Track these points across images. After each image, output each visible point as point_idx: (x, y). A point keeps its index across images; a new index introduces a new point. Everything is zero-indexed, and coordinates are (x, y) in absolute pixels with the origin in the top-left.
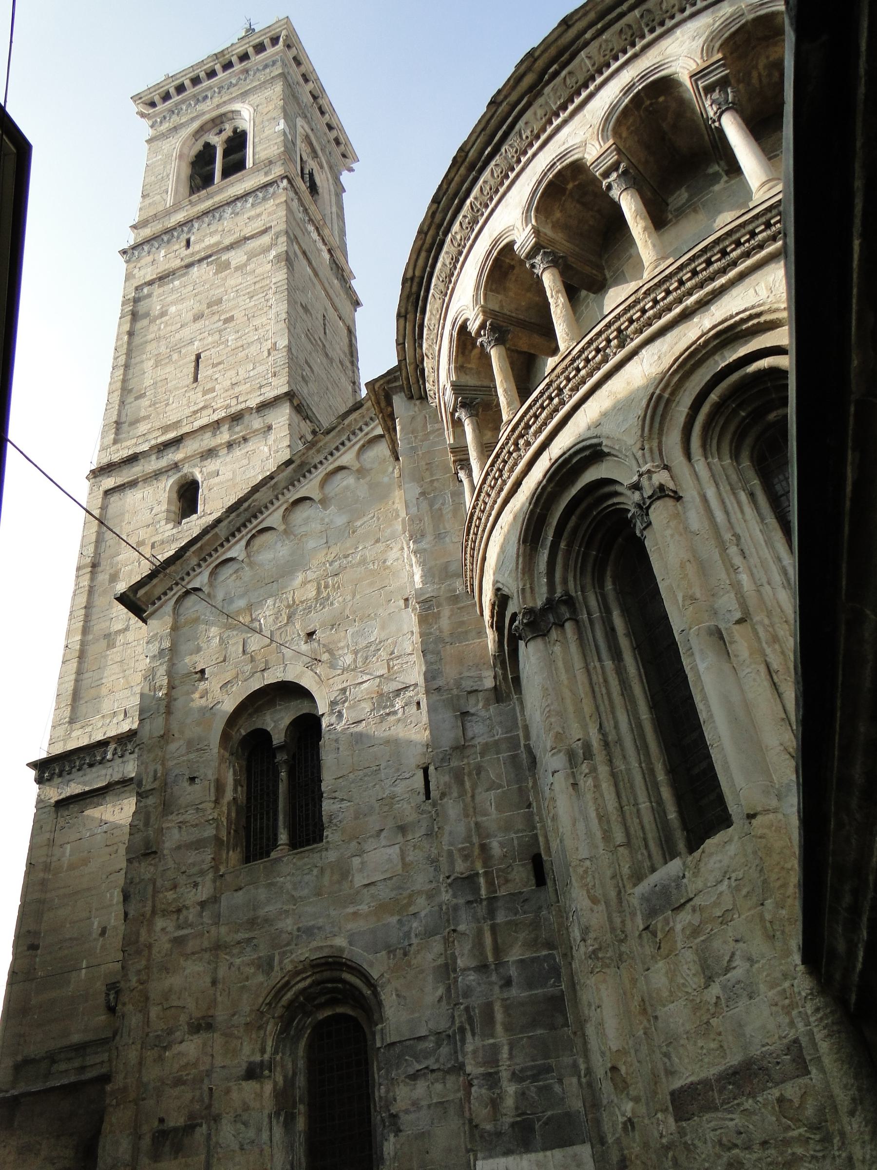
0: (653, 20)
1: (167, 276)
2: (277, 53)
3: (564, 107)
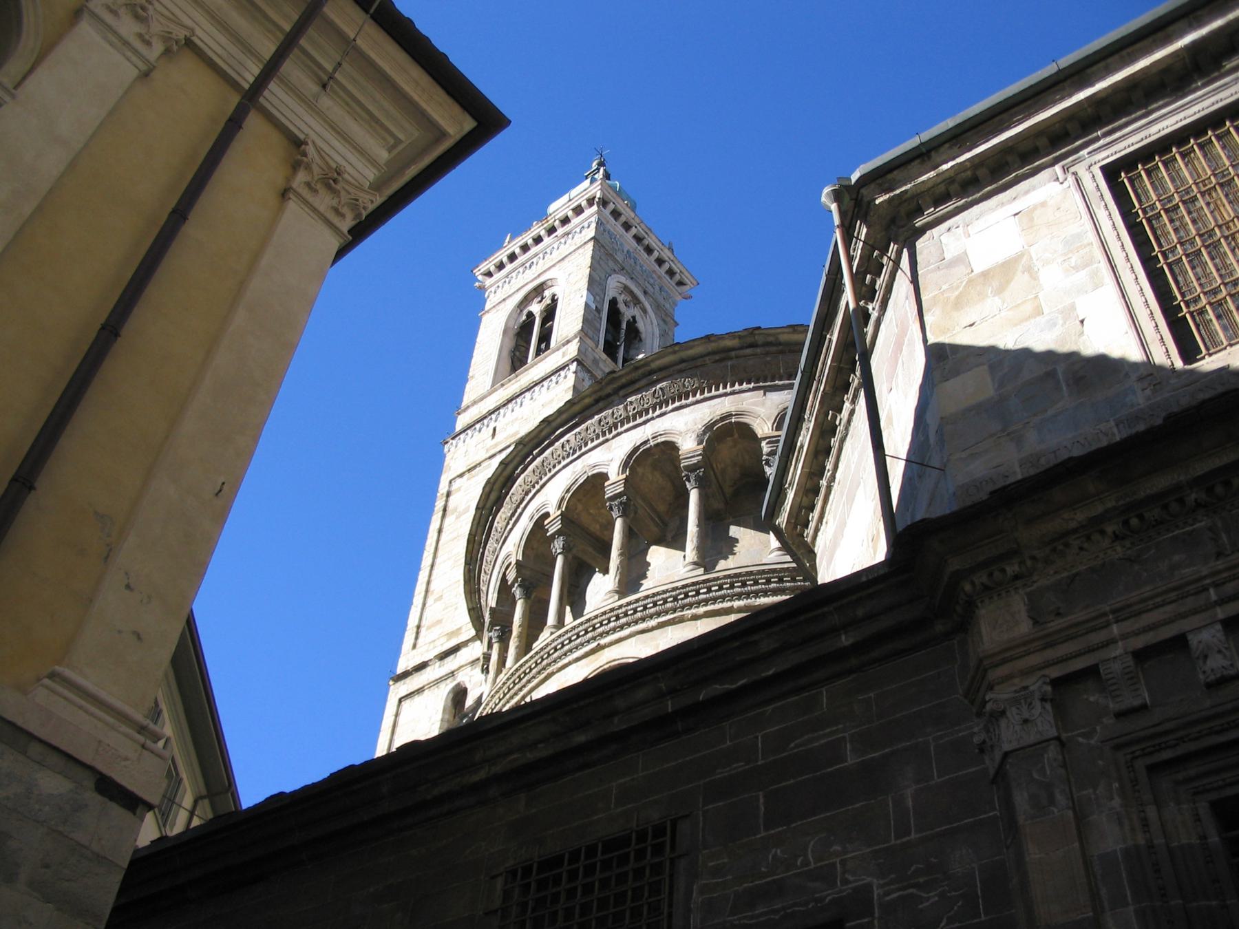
0: (550, 464)
1: (475, 467)
2: (592, 215)
3: (513, 515)
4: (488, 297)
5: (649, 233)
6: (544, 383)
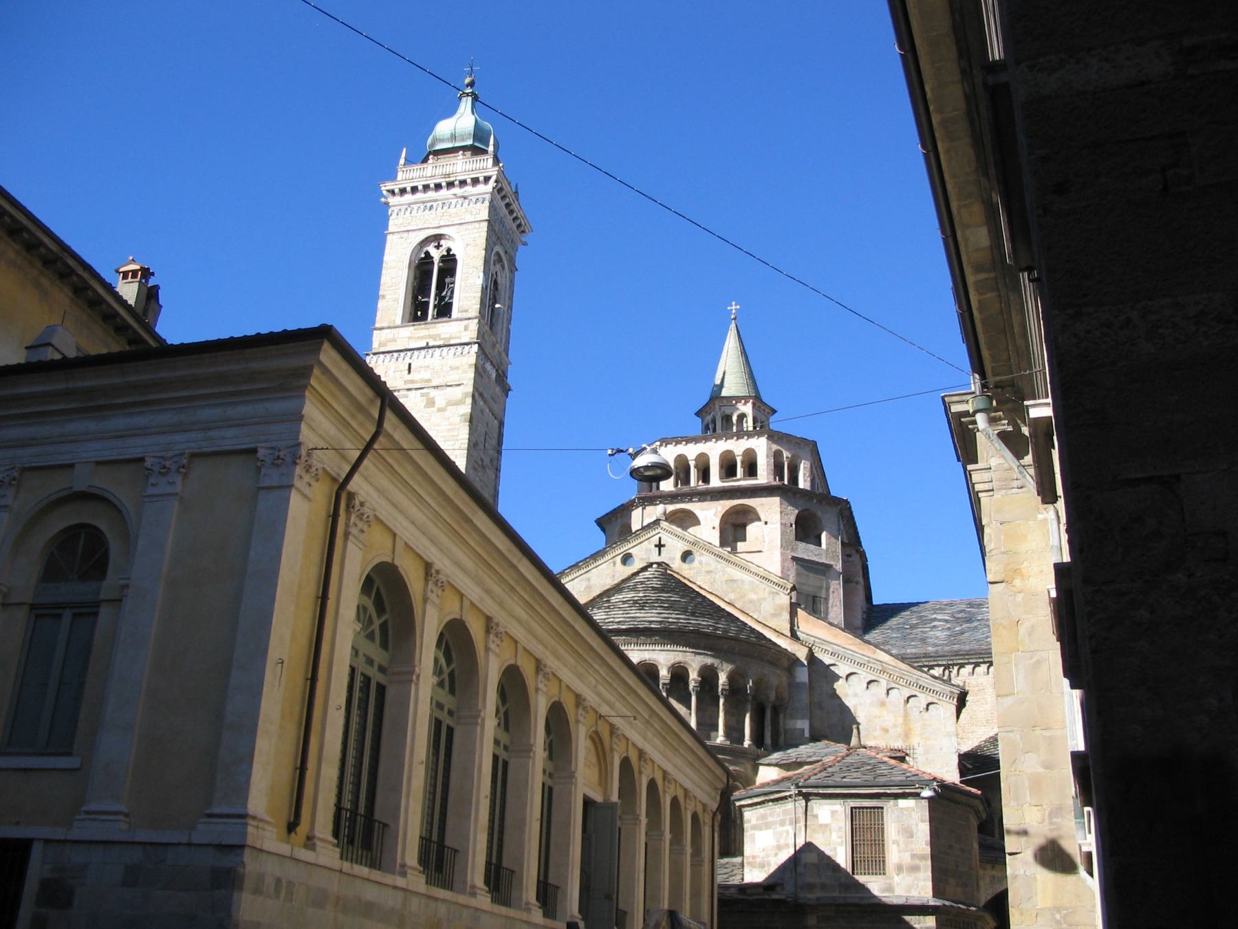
4: (391, 215)
5: (515, 200)
6: (452, 348)
